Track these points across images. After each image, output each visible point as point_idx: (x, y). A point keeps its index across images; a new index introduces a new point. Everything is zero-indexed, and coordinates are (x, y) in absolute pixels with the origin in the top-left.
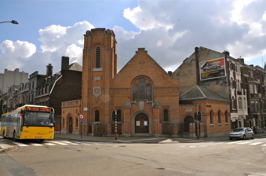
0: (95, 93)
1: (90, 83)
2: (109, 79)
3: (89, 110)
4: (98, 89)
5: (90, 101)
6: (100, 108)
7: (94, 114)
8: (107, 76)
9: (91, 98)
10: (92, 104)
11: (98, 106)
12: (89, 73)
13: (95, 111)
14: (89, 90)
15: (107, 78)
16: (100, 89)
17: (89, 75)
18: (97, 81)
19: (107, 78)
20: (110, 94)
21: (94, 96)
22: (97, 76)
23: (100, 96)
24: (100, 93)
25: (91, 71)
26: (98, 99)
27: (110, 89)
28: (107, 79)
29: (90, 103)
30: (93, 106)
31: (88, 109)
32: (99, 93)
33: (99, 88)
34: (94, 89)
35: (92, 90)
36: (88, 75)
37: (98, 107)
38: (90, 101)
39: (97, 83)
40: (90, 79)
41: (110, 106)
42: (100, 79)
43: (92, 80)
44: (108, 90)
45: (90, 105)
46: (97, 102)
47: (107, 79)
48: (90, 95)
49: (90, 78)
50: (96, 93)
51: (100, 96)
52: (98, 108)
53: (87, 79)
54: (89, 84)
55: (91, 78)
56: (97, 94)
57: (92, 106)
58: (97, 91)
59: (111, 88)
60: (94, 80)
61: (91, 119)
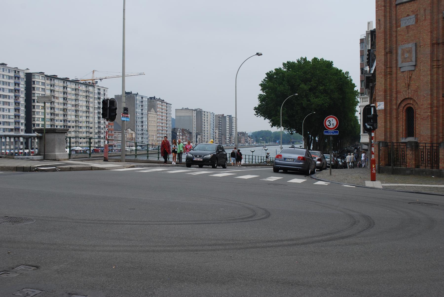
0: (402, 62)
1: (391, 35)
2: (428, 17)
3: (388, 108)
4: (410, 51)
5: (391, 85)
6: (414, 101)
7: (403, 116)
8: (425, 10)
9: (394, 76)
10: (397, 93)
11: (410, 96)
12: (388, 10)
13: (405, 108)
14: (389, 55)
15: (425, 15)
16: (414, 49)
17: (388, 14)
18: (408, 27)
19: (425, 15)
20: (432, 61)
21: (402, 70)
22: (408, 15)
23: (413, 68)
24: (414, 59)
25: (394, 4)
26: (410, 77)
27: (432, 45)
28: (425, 20)
29: (391, 90)
30: (399, 96)
31: (385, 105)
32: (412, 61)
33: (411, 48)
34: (400, 52)
35: (397, 53)
36: (385, 16)
37: (411, 99)
38: (391, 85)
39: (408, 33)
40: (391, 27)
41: (435, 95)
42: (414, 23)
43: (397, 27)
44: (428, 50)
45: (391, 96)
46: (409, 85)
47: (425, 18)
48: (391, 67)
49: (390, 23)
50: (405, 62)
51: (413, 68)
52: (411, 102)
53: (382, 29)
54: (388, 41)
55: (394, 22)
56: (407, 64)
57: (396, 97)
58: (407, 55)
59: (434, 42)
60: (400, 26)
61: (394, 129)
